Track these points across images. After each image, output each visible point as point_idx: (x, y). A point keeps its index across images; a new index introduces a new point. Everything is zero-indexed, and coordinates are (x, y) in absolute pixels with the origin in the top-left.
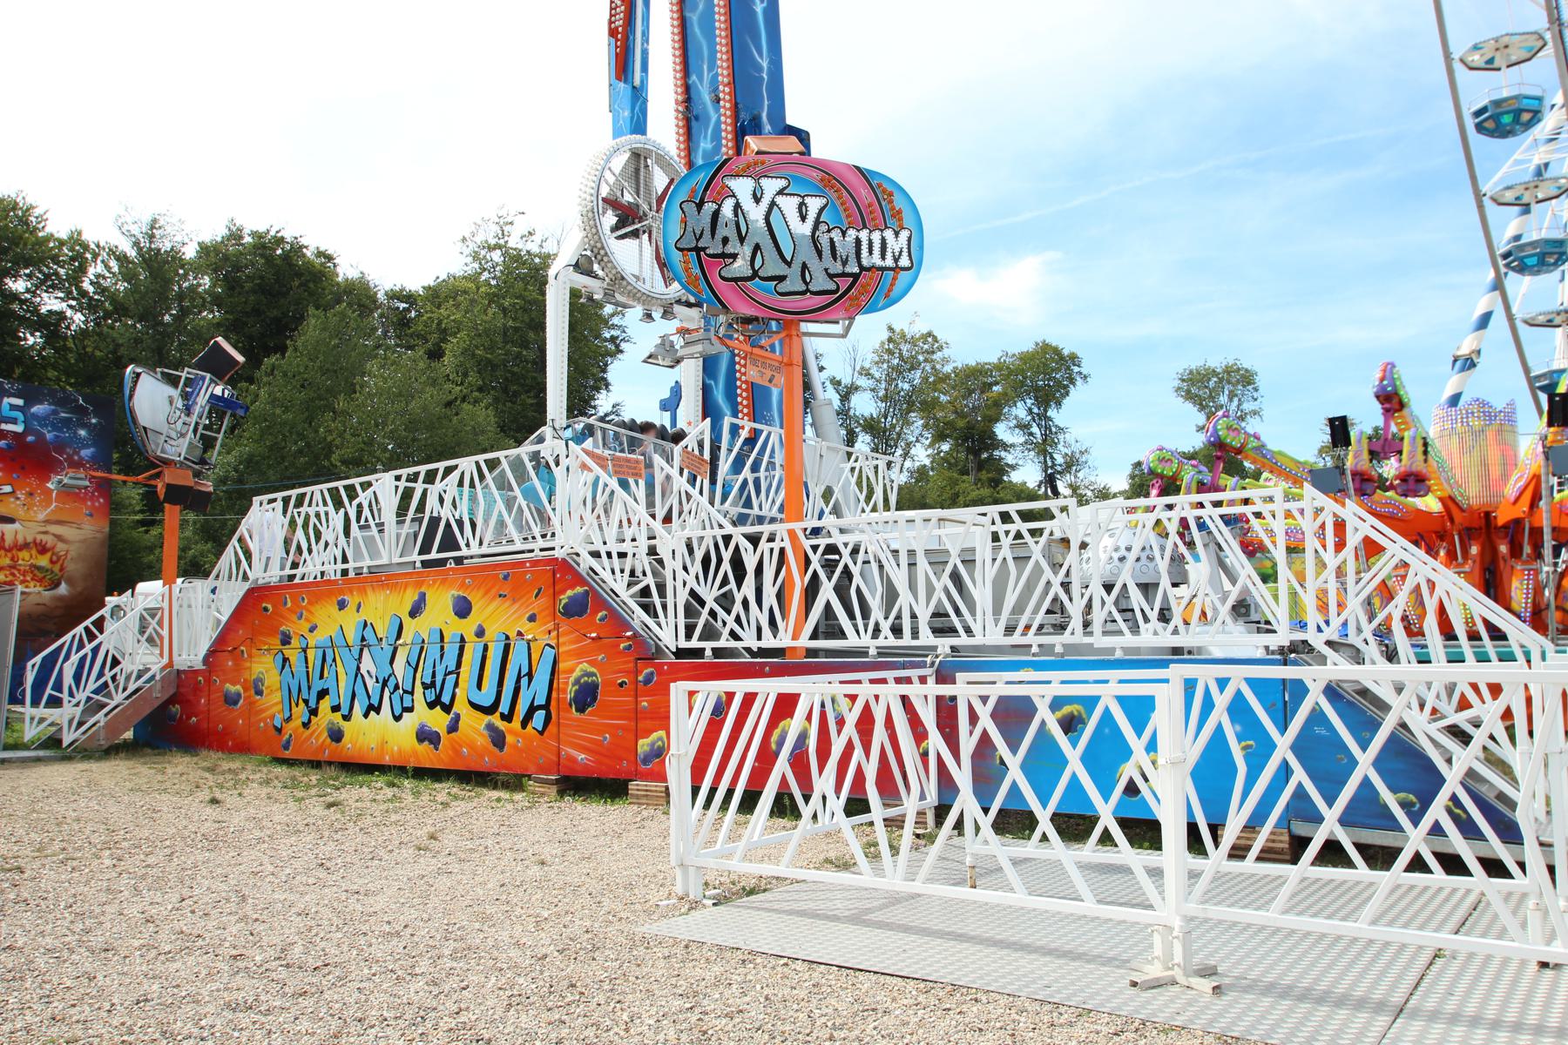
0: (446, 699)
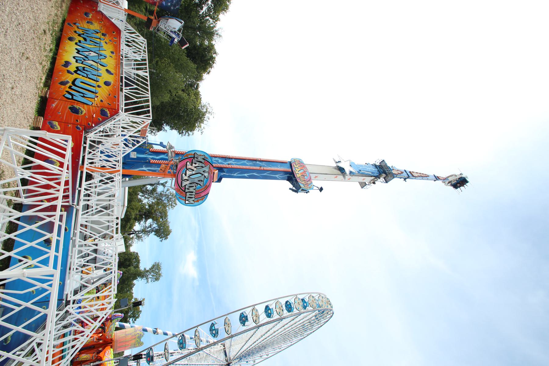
0: (79, 72)
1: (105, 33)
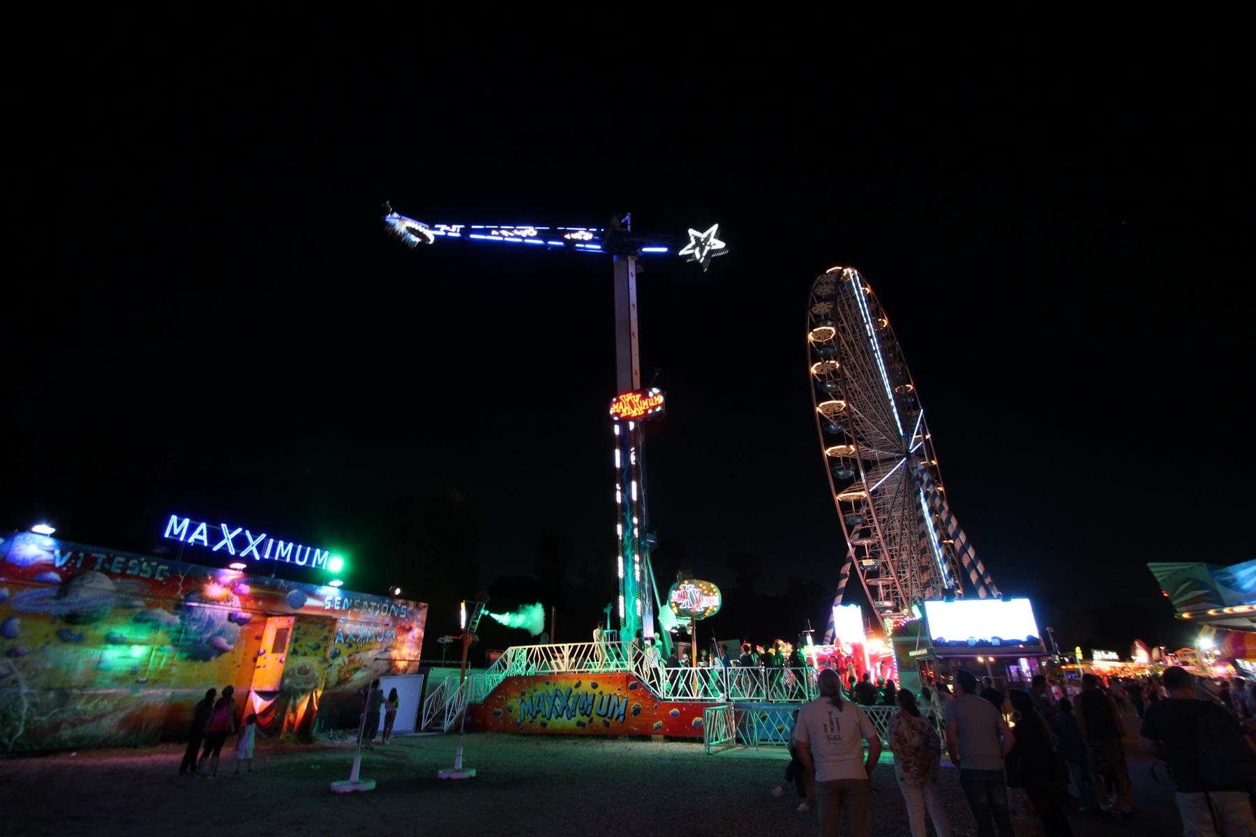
0: (588, 712)
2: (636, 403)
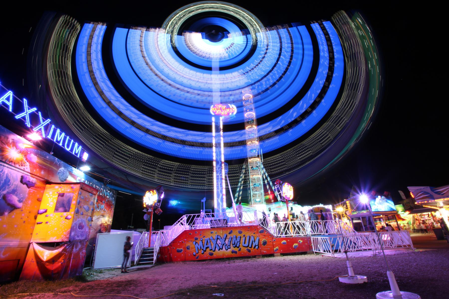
0: (238, 246)
1: (194, 239)
2: (223, 109)
